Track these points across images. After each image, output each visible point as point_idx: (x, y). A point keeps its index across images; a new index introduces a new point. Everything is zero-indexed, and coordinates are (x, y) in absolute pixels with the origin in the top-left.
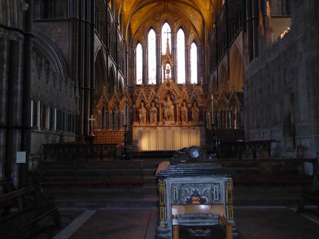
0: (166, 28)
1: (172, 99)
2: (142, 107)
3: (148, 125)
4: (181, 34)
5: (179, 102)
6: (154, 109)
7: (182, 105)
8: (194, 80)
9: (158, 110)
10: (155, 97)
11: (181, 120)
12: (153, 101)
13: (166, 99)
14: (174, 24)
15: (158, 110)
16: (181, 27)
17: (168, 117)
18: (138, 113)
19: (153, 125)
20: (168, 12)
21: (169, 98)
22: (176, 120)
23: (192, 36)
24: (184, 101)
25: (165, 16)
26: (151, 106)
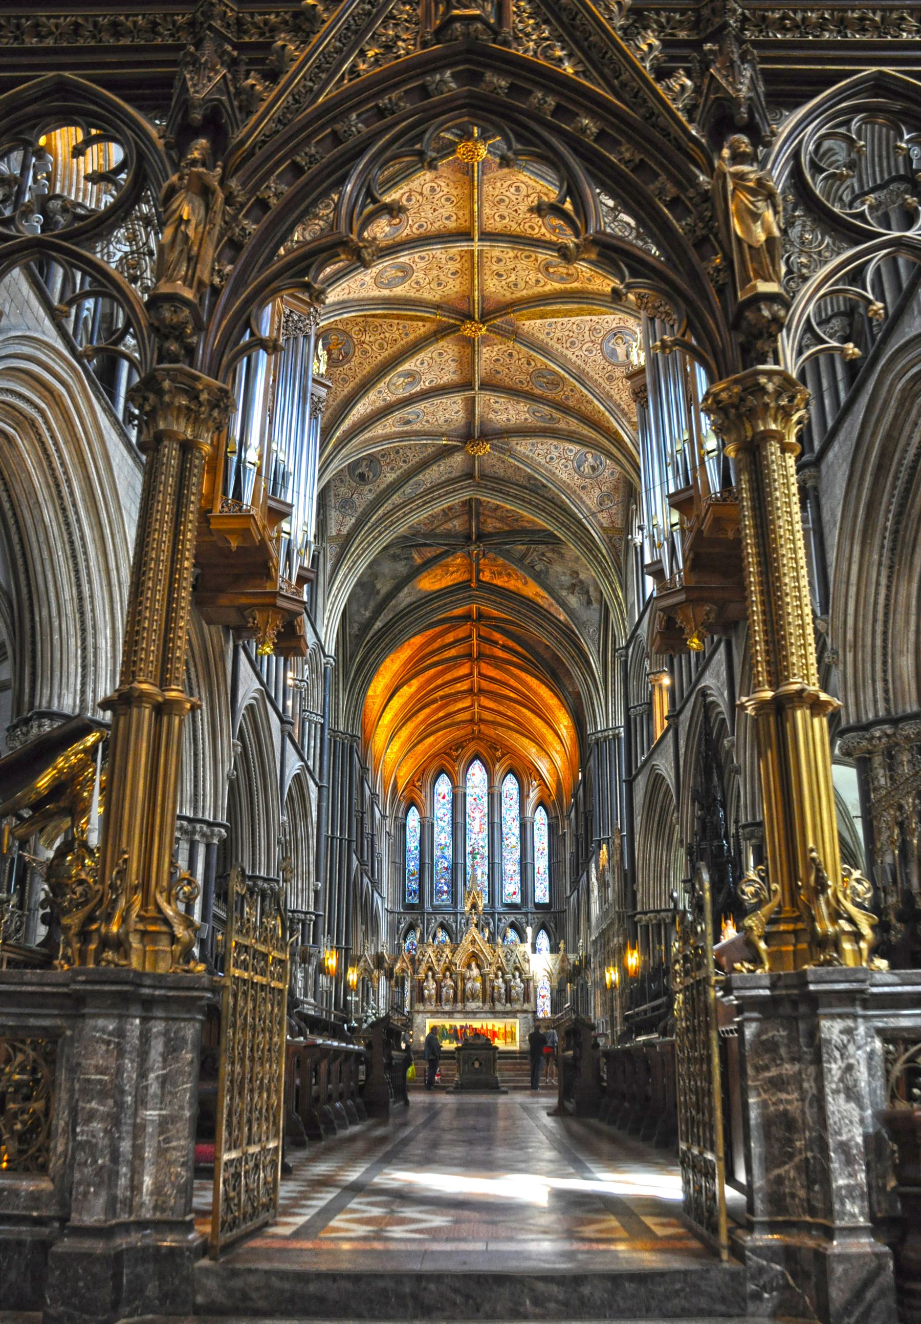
0: (477, 773)
1: (478, 966)
2: (430, 978)
3: (439, 1008)
4: (510, 786)
5: (490, 970)
6: (449, 982)
7: (497, 977)
8: (542, 894)
9: (456, 983)
10: (450, 962)
11: (493, 1001)
12: (448, 969)
13: (469, 967)
14: (494, 765)
15: (456, 983)
16: (511, 771)
17: (473, 995)
18: (422, 989)
19: (447, 1008)
20: (480, 739)
21: (473, 965)
22: (484, 1002)
23: (533, 795)
24: (499, 968)
25: (472, 748)
26: (444, 976)
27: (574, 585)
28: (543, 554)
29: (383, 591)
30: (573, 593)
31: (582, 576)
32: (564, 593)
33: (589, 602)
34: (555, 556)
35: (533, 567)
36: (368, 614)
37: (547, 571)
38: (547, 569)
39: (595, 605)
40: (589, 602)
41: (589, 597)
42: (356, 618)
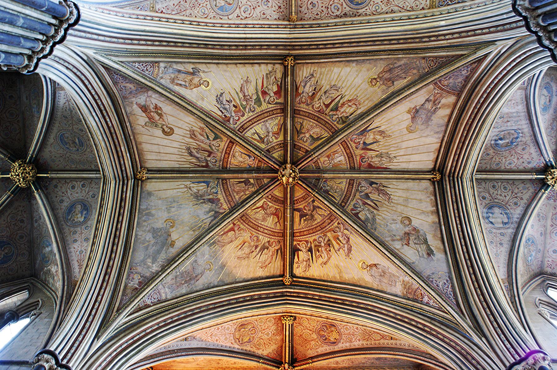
27: (407, 234)
28: (367, 196)
29: (180, 244)
30: (408, 244)
31: (416, 223)
32: (397, 246)
33: (430, 253)
34: (381, 198)
35: (356, 215)
36: (155, 268)
37: (374, 219)
38: (374, 216)
39: (439, 256)
40: (430, 253)
41: (428, 246)
42: (139, 269)
